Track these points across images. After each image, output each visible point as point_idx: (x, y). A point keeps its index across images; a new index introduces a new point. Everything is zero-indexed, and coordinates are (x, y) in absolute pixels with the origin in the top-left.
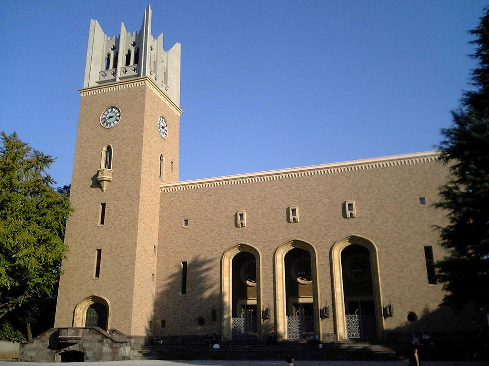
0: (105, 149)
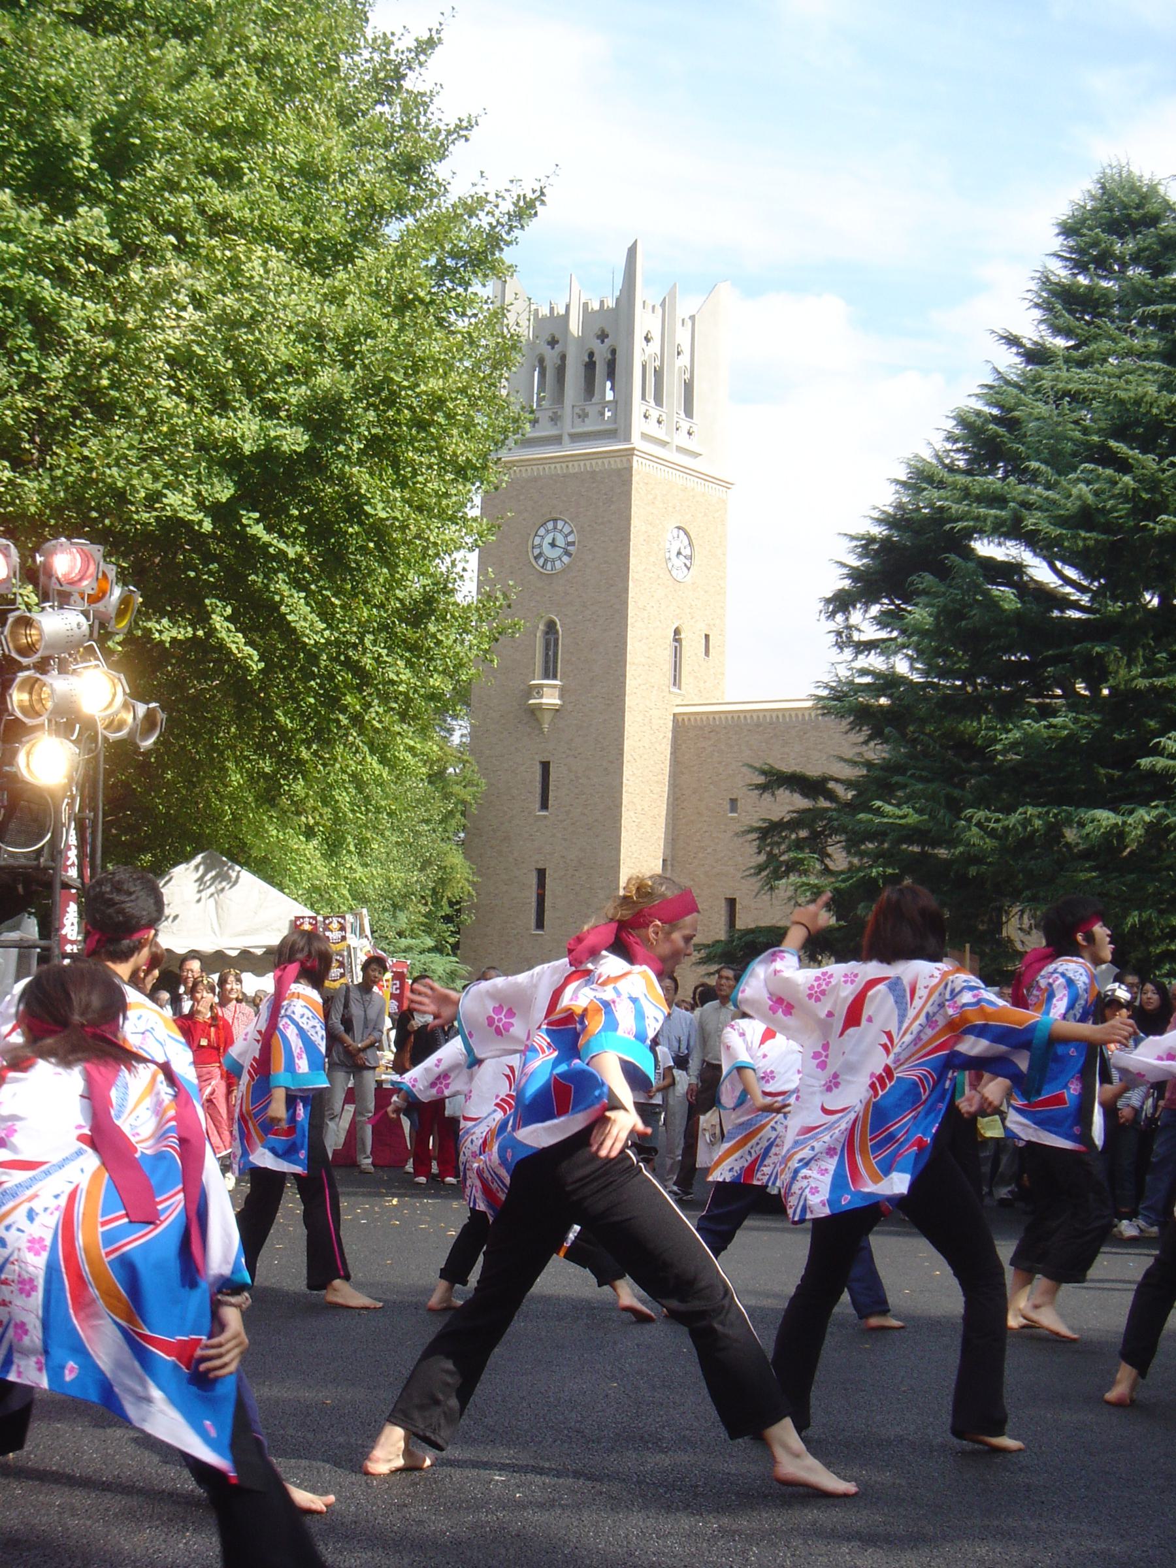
0: (542, 627)
